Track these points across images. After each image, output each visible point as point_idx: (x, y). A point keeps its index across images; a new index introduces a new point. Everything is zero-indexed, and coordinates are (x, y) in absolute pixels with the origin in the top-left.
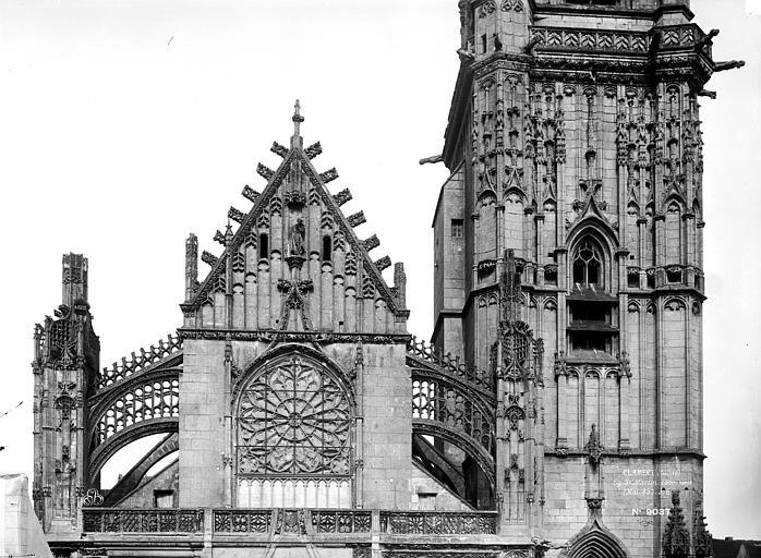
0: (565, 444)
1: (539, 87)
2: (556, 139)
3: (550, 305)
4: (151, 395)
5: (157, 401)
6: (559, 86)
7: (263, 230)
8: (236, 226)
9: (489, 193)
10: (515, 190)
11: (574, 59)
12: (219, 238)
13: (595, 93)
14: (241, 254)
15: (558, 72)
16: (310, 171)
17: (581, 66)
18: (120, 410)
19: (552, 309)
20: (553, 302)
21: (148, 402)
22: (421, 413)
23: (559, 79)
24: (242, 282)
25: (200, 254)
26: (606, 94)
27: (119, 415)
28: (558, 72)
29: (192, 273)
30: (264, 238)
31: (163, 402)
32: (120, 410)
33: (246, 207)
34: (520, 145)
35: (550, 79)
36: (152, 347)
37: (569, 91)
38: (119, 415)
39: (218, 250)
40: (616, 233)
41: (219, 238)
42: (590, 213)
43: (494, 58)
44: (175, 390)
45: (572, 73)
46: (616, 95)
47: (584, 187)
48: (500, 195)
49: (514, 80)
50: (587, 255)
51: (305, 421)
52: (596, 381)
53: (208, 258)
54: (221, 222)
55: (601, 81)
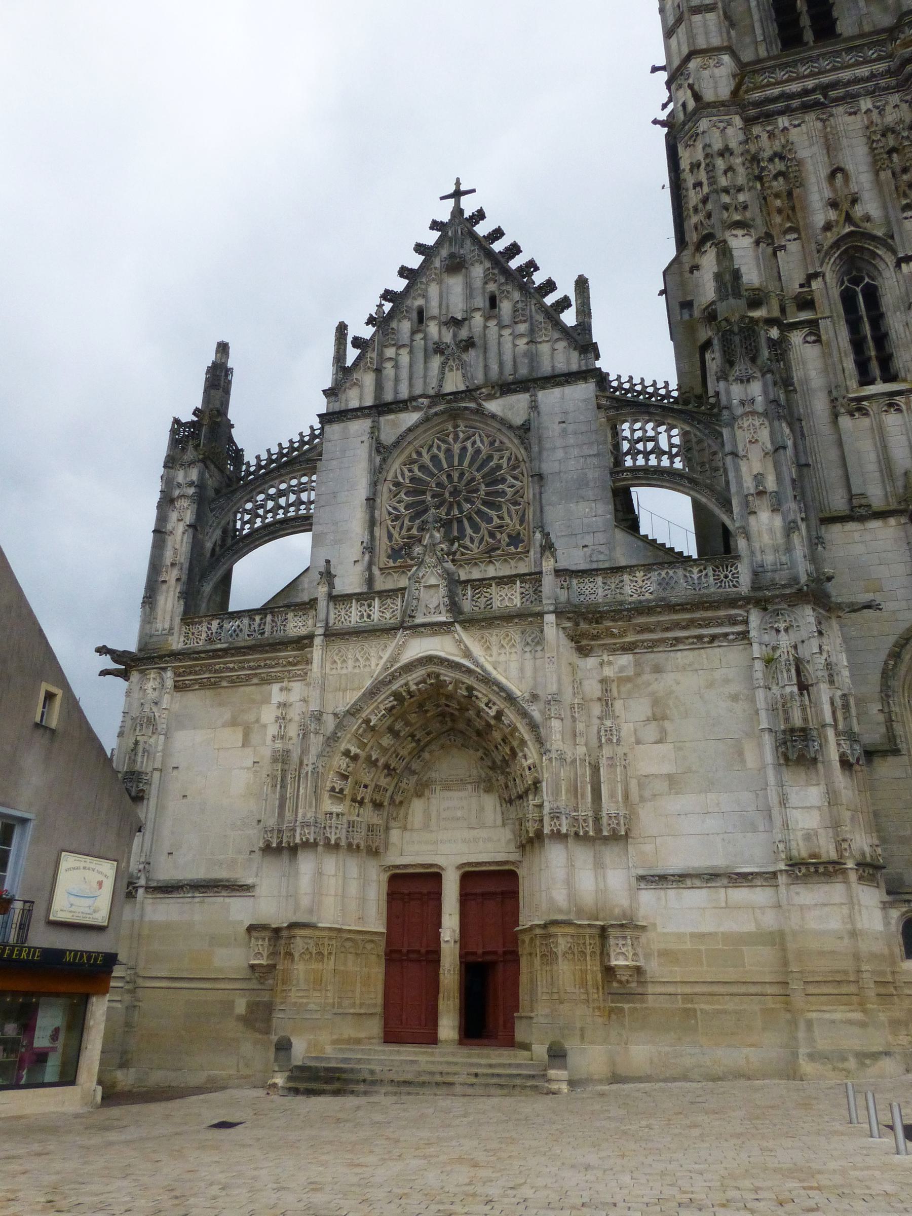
0: (864, 502)
1: (756, 130)
2: (788, 167)
3: (813, 338)
4: (281, 493)
5: (292, 498)
6: (783, 121)
7: (420, 302)
8: (388, 306)
9: (707, 237)
10: (739, 225)
11: (795, 87)
12: (371, 321)
13: (832, 115)
14: (392, 329)
15: (780, 105)
16: (473, 236)
17: (806, 92)
18: (248, 512)
19: (814, 342)
20: (815, 334)
21: (282, 501)
22: (635, 460)
23: (781, 113)
24: (393, 356)
25: (349, 339)
26: (846, 113)
27: (247, 517)
28: (780, 105)
29: (340, 356)
30: (420, 312)
31: (299, 498)
32: (248, 512)
33: (399, 285)
34: (741, 180)
35: (769, 116)
36: (291, 442)
37: (796, 123)
38: (247, 517)
39: (367, 332)
40: (889, 241)
41: (371, 321)
42: (848, 229)
43: (695, 111)
44: (314, 484)
45: (795, 103)
46: (859, 110)
47: (834, 204)
48: (719, 235)
49: (721, 125)
50: (856, 281)
51: (456, 463)
52: (899, 416)
53: (357, 342)
54: (370, 304)
55: (838, 100)
